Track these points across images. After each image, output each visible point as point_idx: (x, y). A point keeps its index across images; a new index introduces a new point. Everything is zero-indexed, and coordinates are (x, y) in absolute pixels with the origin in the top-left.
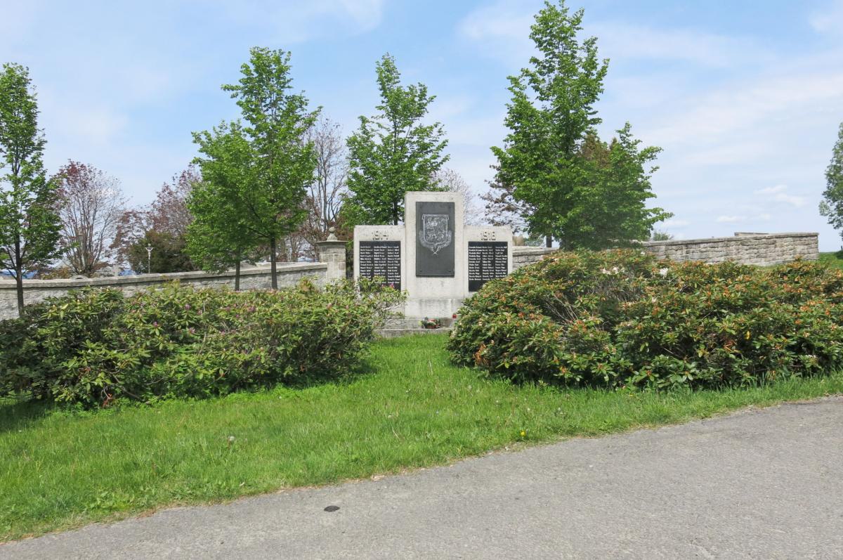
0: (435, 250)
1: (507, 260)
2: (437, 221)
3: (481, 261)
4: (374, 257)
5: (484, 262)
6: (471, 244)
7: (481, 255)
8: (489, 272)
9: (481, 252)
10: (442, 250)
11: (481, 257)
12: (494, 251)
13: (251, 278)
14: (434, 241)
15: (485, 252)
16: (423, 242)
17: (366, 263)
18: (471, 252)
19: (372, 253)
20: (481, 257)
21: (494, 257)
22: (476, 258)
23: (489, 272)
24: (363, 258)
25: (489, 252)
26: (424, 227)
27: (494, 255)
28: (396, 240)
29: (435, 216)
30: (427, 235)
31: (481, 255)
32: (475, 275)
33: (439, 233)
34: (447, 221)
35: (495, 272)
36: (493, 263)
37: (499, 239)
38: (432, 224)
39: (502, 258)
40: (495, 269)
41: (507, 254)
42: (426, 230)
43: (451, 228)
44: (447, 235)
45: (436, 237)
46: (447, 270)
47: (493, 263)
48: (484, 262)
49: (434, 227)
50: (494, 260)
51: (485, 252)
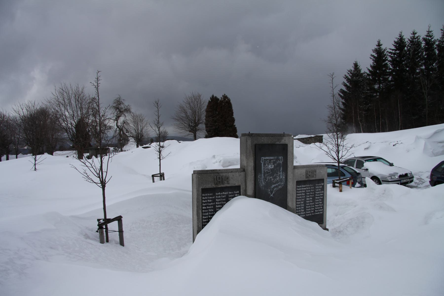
0: (272, 192)
2: (274, 163)
4: (215, 205)
6: (299, 183)
9: (306, 190)
11: (306, 195)
12: (315, 189)
14: (271, 183)
15: (308, 190)
17: (208, 212)
18: (298, 191)
19: (214, 201)
20: (306, 195)
22: (302, 196)
24: (205, 206)
26: (263, 170)
27: (315, 192)
34: (281, 162)
36: (314, 199)
38: (270, 166)
41: (323, 191)
45: (272, 180)
47: (314, 199)
48: (308, 199)
49: (271, 169)
51: (308, 190)
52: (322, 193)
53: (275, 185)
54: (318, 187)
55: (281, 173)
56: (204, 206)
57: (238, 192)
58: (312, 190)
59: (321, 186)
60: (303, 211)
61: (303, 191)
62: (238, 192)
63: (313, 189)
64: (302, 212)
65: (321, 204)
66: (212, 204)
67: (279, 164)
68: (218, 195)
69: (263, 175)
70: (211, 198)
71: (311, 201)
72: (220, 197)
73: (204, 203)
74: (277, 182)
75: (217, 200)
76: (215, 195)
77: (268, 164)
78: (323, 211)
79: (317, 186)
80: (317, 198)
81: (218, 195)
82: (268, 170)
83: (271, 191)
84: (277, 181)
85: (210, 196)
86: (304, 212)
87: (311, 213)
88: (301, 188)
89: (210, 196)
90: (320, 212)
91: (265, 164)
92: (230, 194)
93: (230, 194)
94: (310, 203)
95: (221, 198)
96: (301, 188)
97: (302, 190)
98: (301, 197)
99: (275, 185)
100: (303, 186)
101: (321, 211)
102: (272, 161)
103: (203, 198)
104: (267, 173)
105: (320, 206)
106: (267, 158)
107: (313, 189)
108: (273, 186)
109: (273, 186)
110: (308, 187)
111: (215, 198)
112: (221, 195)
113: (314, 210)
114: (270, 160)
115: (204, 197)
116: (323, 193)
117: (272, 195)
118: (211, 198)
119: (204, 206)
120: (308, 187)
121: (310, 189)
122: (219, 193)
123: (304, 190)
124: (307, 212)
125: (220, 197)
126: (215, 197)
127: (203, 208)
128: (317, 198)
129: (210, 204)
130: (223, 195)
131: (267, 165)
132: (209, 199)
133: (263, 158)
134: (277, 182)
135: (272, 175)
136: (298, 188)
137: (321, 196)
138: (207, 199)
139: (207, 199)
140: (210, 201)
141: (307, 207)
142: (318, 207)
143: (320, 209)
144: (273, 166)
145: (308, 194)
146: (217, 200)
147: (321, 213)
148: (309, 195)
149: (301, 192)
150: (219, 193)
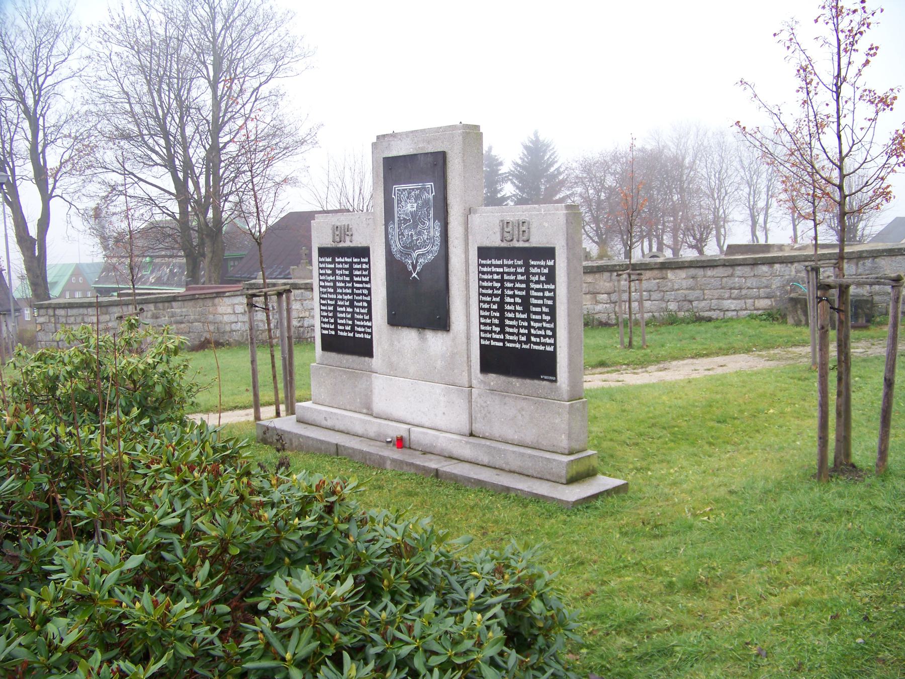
0: (414, 267)
1: (553, 298)
2: (417, 198)
3: (502, 296)
6: (484, 253)
9: (502, 274)
10: (426, 267)
12: (527, 273)
13: (765, 268)
15: (509, 274)
16: (394, 249)
22: (492, 288)
27: (528, 282)
32: (491, 332)
33: (420, 226)
34: (431, 196)
37: (537, 240)
39: (543, 290)
41: (554, 283)
44: (432, 234)
45: (415, 238)
46: (439, 321)
47: (526, 303)
49: (411, 213)
51: (509, 274)
52: (550, 290)
59: (545, 267)
63: (522, 274)
67: (426, 202)
69: (396, 226)
79: (534, 266)
84: (425, 241)
87: (520, 342)
88: (490, 266)
90: (544, 344)
91: (399, 202)
96: (490, 266)
97: (492, 273)
101: (550, 344)
102: (413, 194)
105: (546, 329)
106: (403, 187)
110: (509, 266)
113: (529, 335)
116: (554, 290)
117: (414, 275)
120: (509, 266)
123: (498, 273)
135: (415, 226)
136: (483, 266)
137: (549, 298)
142: (540, 329)
149: (490, 277)
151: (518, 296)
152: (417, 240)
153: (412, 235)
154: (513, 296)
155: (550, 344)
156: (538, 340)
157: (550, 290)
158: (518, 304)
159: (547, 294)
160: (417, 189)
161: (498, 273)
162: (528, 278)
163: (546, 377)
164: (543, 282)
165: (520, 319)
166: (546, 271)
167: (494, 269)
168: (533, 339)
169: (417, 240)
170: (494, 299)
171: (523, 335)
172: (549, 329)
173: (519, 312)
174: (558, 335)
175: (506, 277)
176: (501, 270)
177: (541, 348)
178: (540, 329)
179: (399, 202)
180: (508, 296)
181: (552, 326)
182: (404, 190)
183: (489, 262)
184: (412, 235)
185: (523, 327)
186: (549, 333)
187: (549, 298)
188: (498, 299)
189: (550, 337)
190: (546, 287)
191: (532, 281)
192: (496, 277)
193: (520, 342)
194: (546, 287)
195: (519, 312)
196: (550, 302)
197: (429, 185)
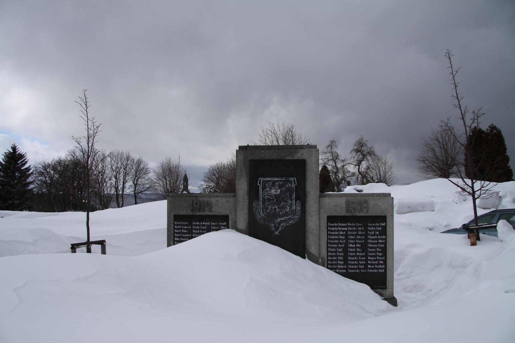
0: (277, 229)
2: (280, 187)
3: (346, 244)
5: (351, 245)
6: (331, 219)
7: (346, 235)
8: (358, 260)
9: (347, 231)
11: (347, 239)
12: (366, 230)
14: (276, 215)
20: (347, 239)
21: (366, 239)
22: (339, 239)
23: (358, 260)
24: (178, 237)
25: (357, 231)
27: (366, 235)
28: (223, 213)
29: (276, 179)
30: (265, 208)
31: (346, 235)
35: (367, 260)
36: (364, 247)
38: (273, 191)
39: (378, 239)
40: (366, 256)
41: (386, 235)
42: (264, 201)
43: (301, 196)
44: (294, 207)
45: (278, 210)
47: (364, 247)
48: (351, 245)
49: (275, 195)
50: (367, 243)
52: (382, 239)
53: (283, 219)
54: (372, 228)
55: (294, 202)
56: (176, 237)
57: (225, 224)
58: (360, 233)
59: (379, 227)
60: (342, 263)
61: (341, 233)
62: (225, 224)
63: (362, 231)
64: (340, 265)
65: (382, 256)
66: (187, 235)
67: (290, 189)
68: (196, 225)
70: (185, 227)
71: (358, 250)
72: (198, 227)
73: (177, 233)
74: (287, 214)
75: (194, 231)
76: (192, 225)
77: (270, 188)
78: (385, 268)
79: (371, 227)
80: (370, 245)
81: (196, 225)
82: (270, 196)
83: (275, 226)
85: (184, 225)
86: (343, 265)
87: (359, 269)
88: (337, 227)
89: (184, 225)
91: (264, 188)
92: (214, 226)
93: (214, 226)
94: (356, 252)
95: (200, 229)
96: (337, 227)
97: (338, 231)
98: (336, 241)
99: (283, 219)
100: (340, 224)
101: (382, 269)
103: (175, 227)
104: (269, 200)
105: (379, 260)
107: (362, 231)
108: (279, 219)
109: (279, 219)
111: (192, 229)
112: (199, 225)
113: (366, 265)
114: (274, 182)
115: (177, 225)
116: (386, 239)
117: (277, 233)
118: (185, 227)
119: (176, 237)
120: (351, 227)
121: (357, 231)
122: (198, 223)
123: (343, 231)
124: (350, 266)
125: (198, 227)
126: (192, 227)
127: (176, 239)
128: (370, 245)
129: (185, 236)
130: (203, 225)
131: (268, 189)
132: (184, 229)
133: (262, 179)
134: (287, 214)
135: (278, 203)
136: (331, 227)
137: (381, 243)
138: (181, 229)
139: (181, 229)
140: (185, 231)
141: (350, 258)
142: (374, 260)
143: (378, 264)
144: (279, 191)
145: (352, 237)
146: (194, 231)
147: (380, 271)
148: (353, 239)
150: (198, 223)
151: (359, 243)
152: (280, 212)
153: (275, 209)
154: (355, 243)
155: (382, 269)
156: (373, 267)
157: (382, 239)
158: (358, 247)
159: (380, 241)
160: (281, 181)
161: (343, 231)
162: (366, 233)
163: (379, 287)
164: (377, 235)
165: (359, 256)
166: (380, 229)
167: (340, 229)
168: (369, 266)
169: (280, 212)
170: (340, 246)
171: (362, 264)
172: (381, 260)
173: (359, 252)
174: (387, 263)
175: (349, 233)
176: (346, 229)
177: (375, 271)
178: (374, 260)
179: (264, 188)
180: (350, 243)
181: (384, 258)
182: (269, 181)
183: (336, 225)
184: (275, 209)
185: (361, 260)
186: (381, 262)
187: (381, 243)
188: (343, 246)
189: (381, 265)
190: (379, 237)
191: (369, 235)
192: (341, 233)
193: (359, 269)
194: (379, 237)
195: (359, 252)
196: (382, 246)
197: (292, 179)
